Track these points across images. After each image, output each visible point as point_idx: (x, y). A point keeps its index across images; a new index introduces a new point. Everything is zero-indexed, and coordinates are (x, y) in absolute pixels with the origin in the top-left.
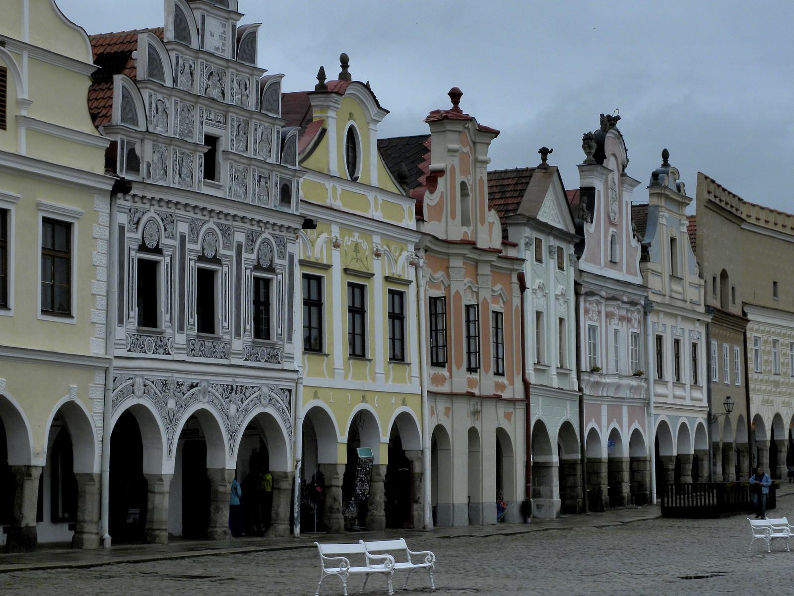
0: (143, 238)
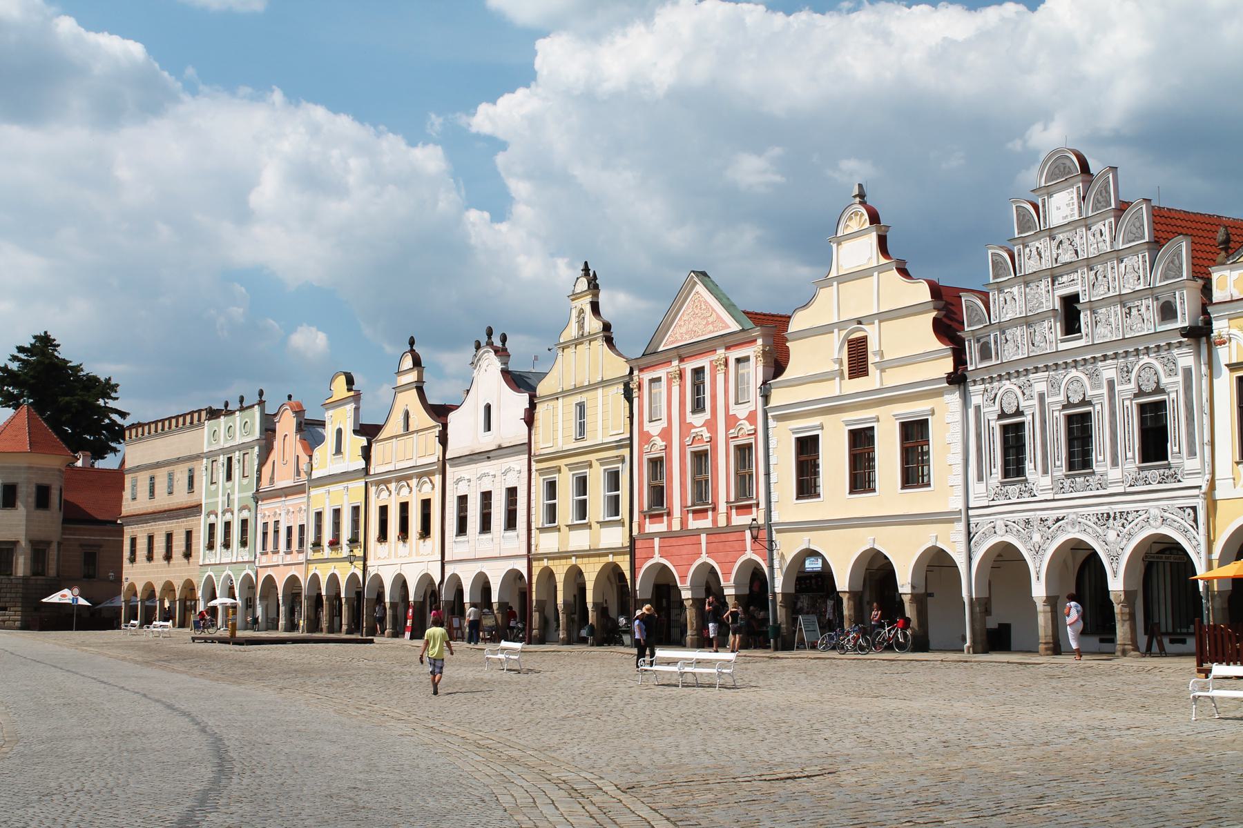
0: (1002, 408)
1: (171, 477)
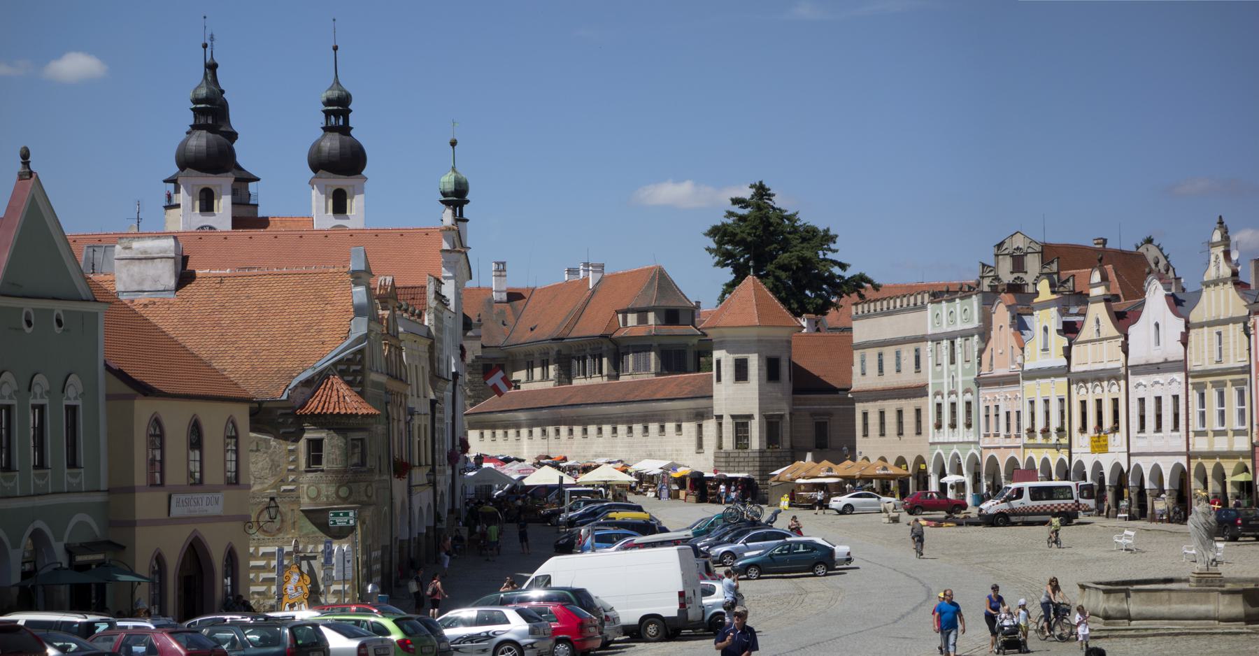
1: (898, 354)
